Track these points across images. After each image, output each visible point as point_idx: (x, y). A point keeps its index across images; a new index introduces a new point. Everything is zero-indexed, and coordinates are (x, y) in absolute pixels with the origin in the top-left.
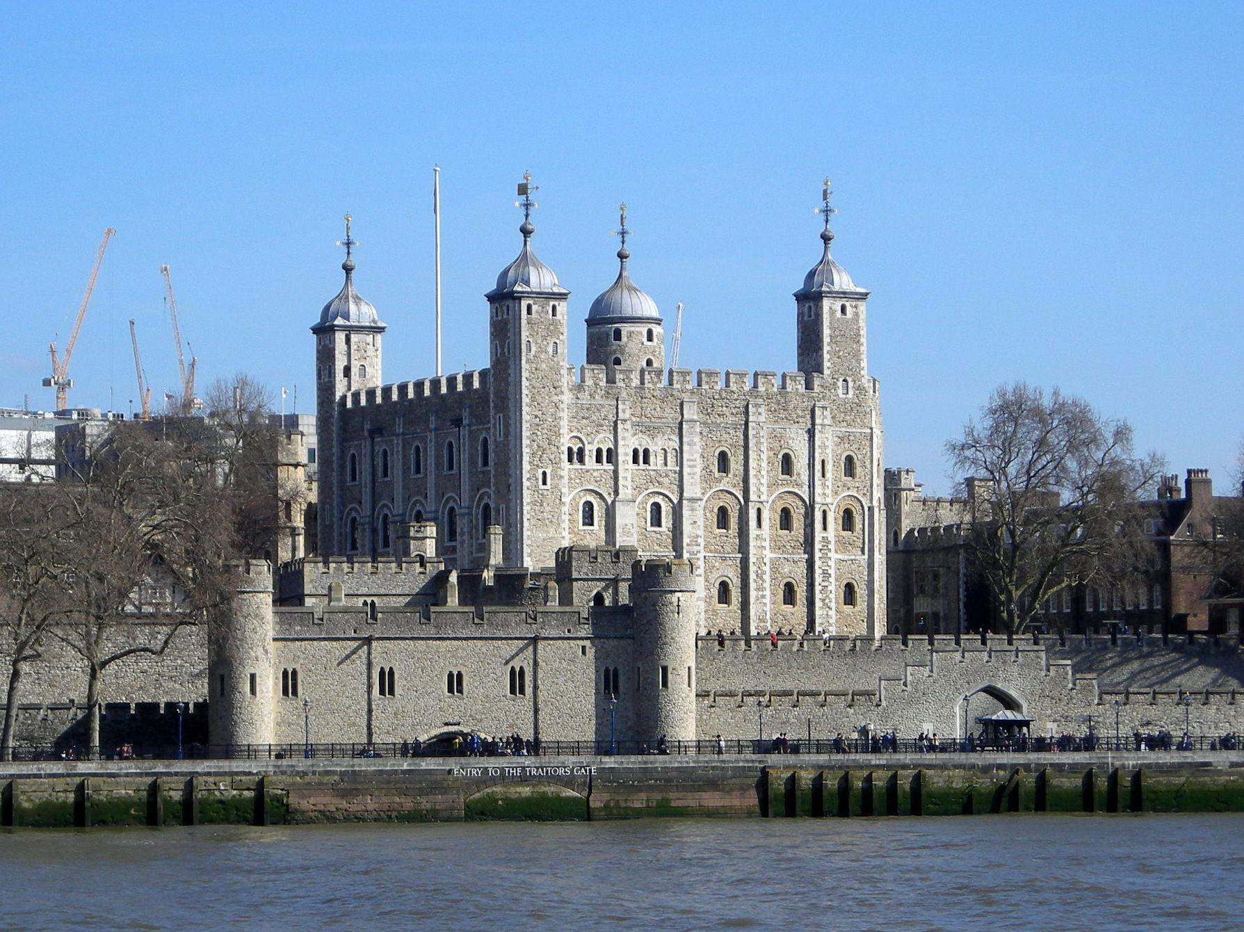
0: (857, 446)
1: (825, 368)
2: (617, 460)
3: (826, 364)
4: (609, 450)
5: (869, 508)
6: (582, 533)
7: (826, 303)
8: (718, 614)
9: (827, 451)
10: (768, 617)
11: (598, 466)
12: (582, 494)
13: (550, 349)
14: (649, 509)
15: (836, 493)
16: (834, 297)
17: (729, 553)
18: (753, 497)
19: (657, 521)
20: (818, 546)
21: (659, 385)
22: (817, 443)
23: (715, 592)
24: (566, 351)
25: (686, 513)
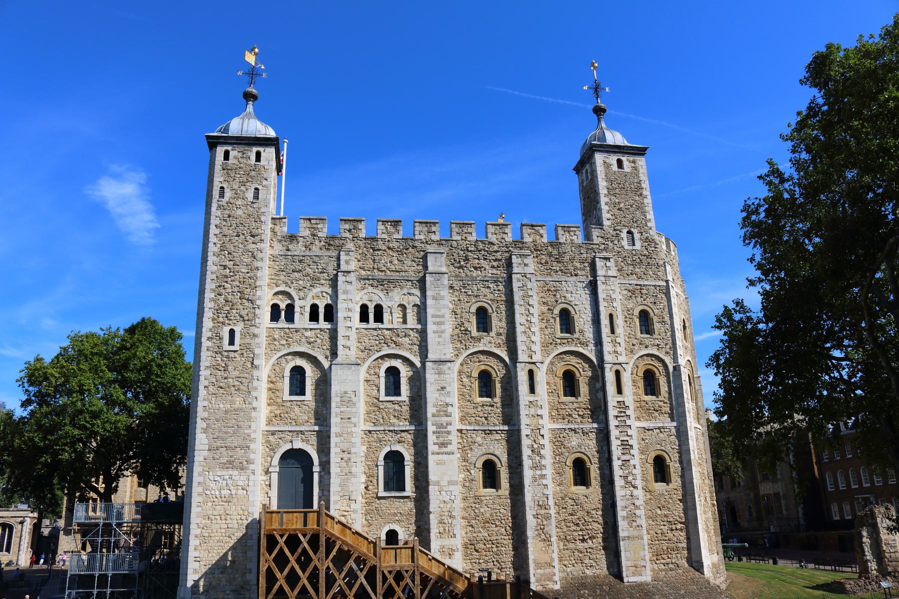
0: (652, 300)
1: (604, 219)
7: (599, 158)
8: (482, 501)
9: (615, 304)
10: (551, 502)
11: (313, 325)
12: (290, 357)
13: (250, 195)
14: (382, 374)
15: (632, 352)
16: (607, 152)
17: (495, 425)
18: (522, 357)
19: (393, 388)
20: (612, 412)
21: (396, 236)
22: (601, 295)
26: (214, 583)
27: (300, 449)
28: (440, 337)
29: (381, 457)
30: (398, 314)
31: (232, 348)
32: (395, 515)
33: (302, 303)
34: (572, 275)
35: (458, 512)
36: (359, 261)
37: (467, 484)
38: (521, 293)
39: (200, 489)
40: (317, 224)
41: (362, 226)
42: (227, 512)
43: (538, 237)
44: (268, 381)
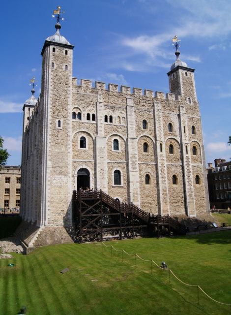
2: (97, 119)
3: (182, 92)
4: (94, 115)
5: (202, 146)
7: (180, 71)
11: (88, 121)
12: (80, 133)
13: (64, 67)
14: (113, 142)
16: (183, 69)
18: (158, 139)
19: (116, 147)
20: (185, 160)
22: (182, 120)
23: (144, 179)
24: (72, 69)
25: (129, 144)
26: (56, 219)
29: (113, 172)
30: (118, 120)
31: (60, 128)
32: (118, 193)
35: (139, 193)
41: (104, 85)
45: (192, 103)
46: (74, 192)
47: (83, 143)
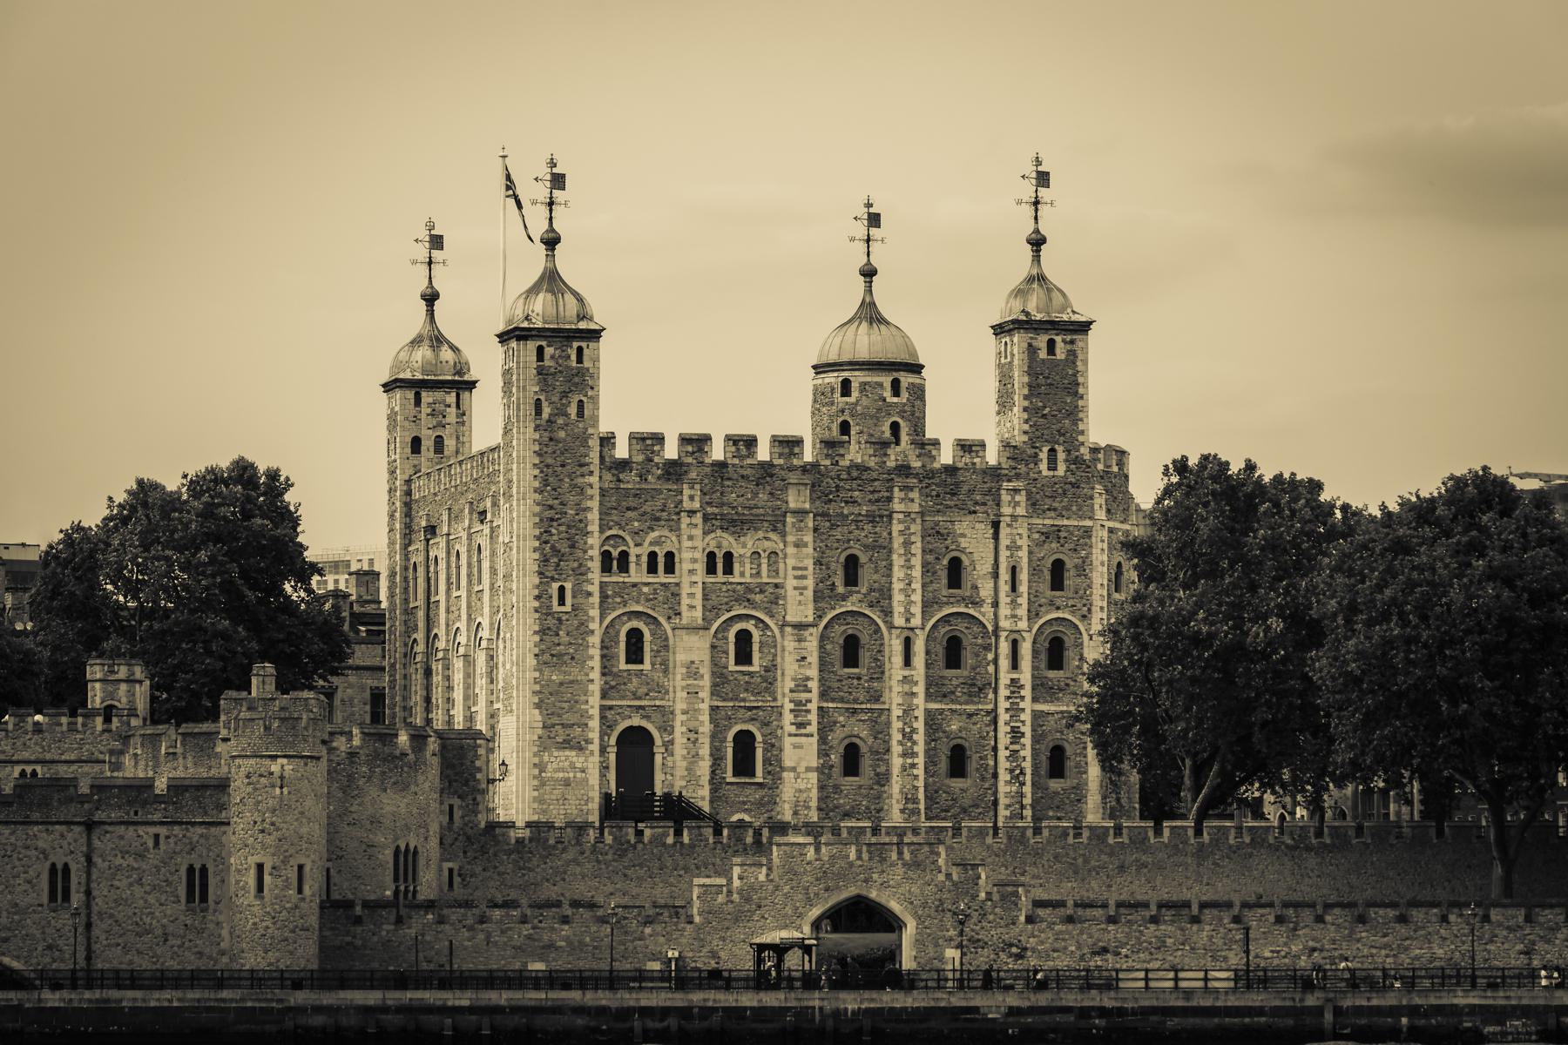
0: (1072, 546)
6: (625, 674)
10: (921, 796)
12: (625, 618)
13: (573, 410)
15: (1037, 614)
16: (1035, 329)
17: (862, 703)
18: (899, 621)
19: (744, 656)
20: (1003, 692)
21: (749, 461)
22: (1004, 541)
27: (640, 727)
28: (801, 594)
32: (744, 803)
33: (638, 550)
34: (970, 513)
35: (814, 804)
36: (705, 494)
37: (826, 771)
38: (901, 540)
39: (536, 772)
40: (653, 445)
42: (567, 796)
43: (926, 459)
44: (602, 648)
45: (1061, 469)
46: (606, 797)
47: (635, 654)
